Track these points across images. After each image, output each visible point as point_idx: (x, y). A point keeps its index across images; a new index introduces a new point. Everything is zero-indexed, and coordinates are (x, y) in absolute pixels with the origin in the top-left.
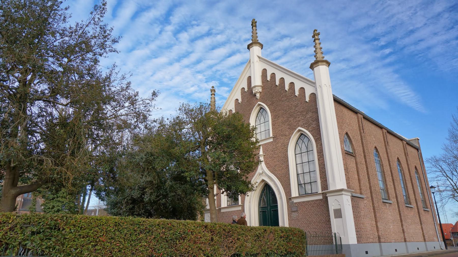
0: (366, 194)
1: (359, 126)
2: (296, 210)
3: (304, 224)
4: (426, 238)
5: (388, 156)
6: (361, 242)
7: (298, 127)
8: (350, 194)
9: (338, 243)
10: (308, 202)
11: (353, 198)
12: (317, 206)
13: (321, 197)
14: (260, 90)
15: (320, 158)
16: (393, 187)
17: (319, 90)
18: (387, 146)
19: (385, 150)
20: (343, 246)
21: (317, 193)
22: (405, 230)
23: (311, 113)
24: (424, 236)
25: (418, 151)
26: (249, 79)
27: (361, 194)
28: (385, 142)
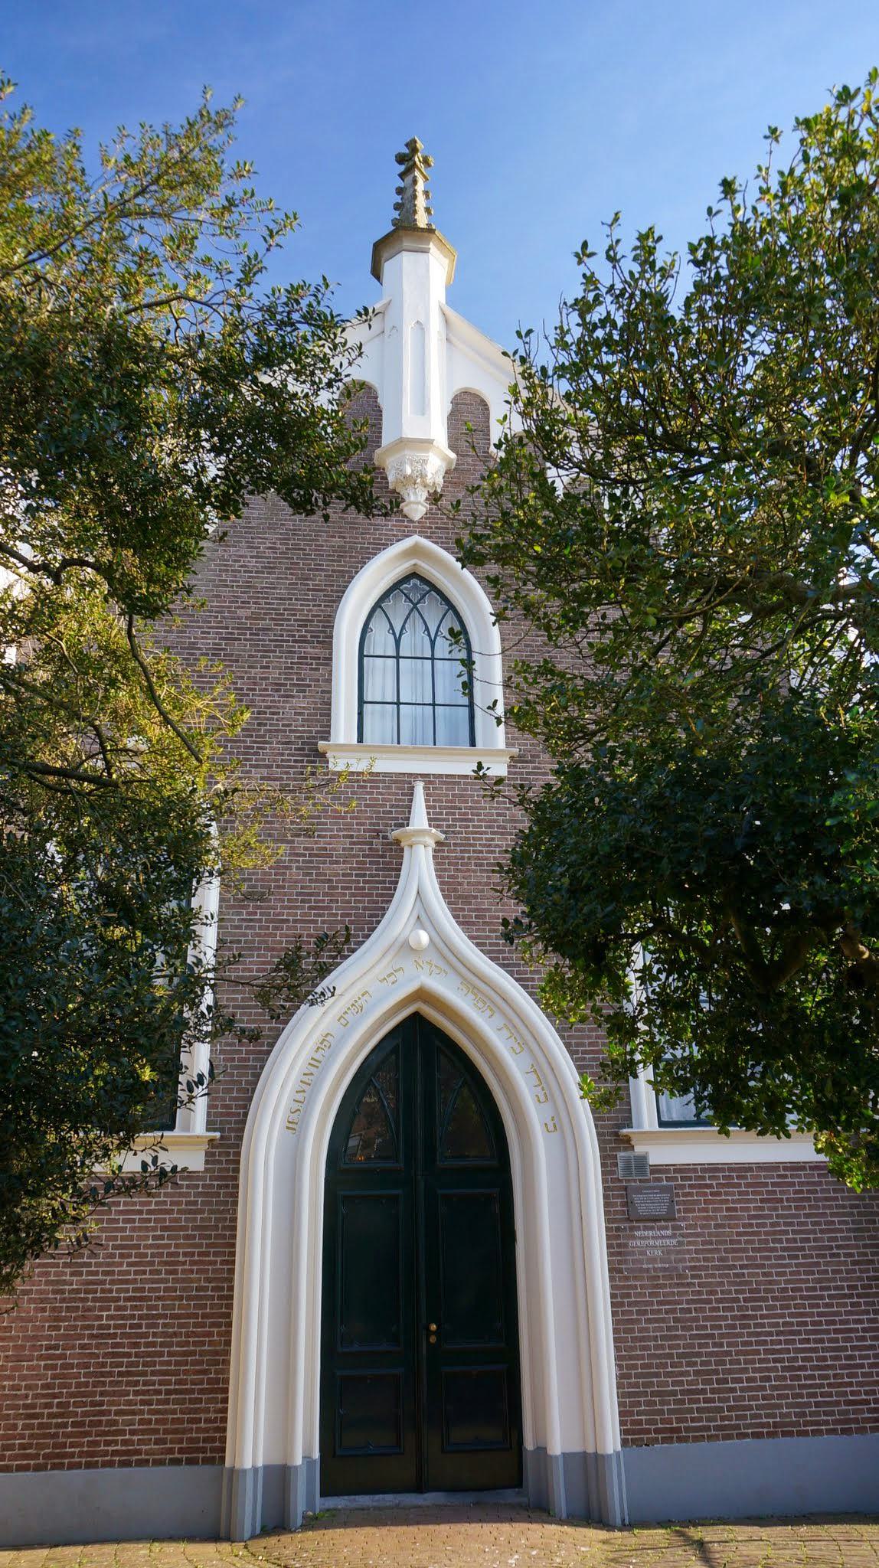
2: (663, 1210)
3: (719, 1301)
10: (742, 1169)
12: (795, 1200)
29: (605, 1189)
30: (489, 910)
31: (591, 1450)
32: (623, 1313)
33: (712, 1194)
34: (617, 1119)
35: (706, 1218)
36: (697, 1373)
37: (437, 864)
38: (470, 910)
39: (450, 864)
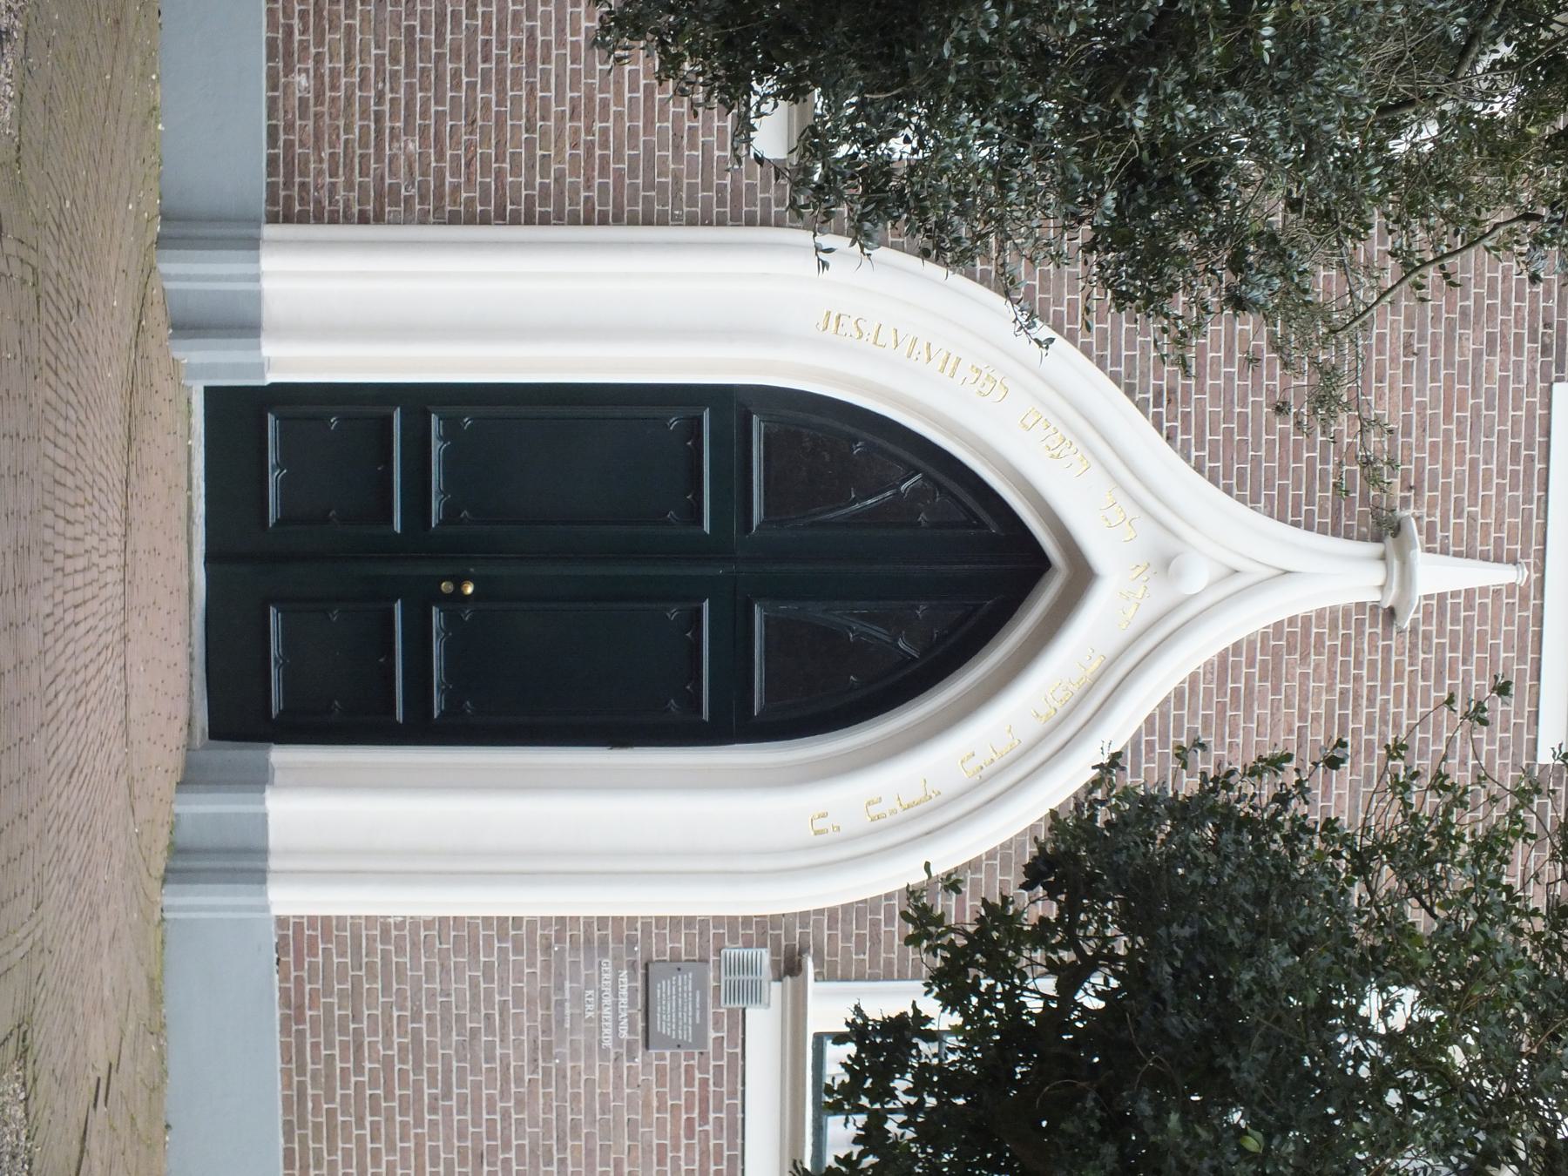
2: (663, 1024)
3: (506, 1114)
29: (704, 922)
30: (1248, 719)
31: (273, 863)
32: (488, 939)
33: (690, 1121)
34: (833, 953)
35: (647, 1105)
36: (388, 1062)
37: (1347, 611)
38: (1249, 677)
39: (1346, 637)
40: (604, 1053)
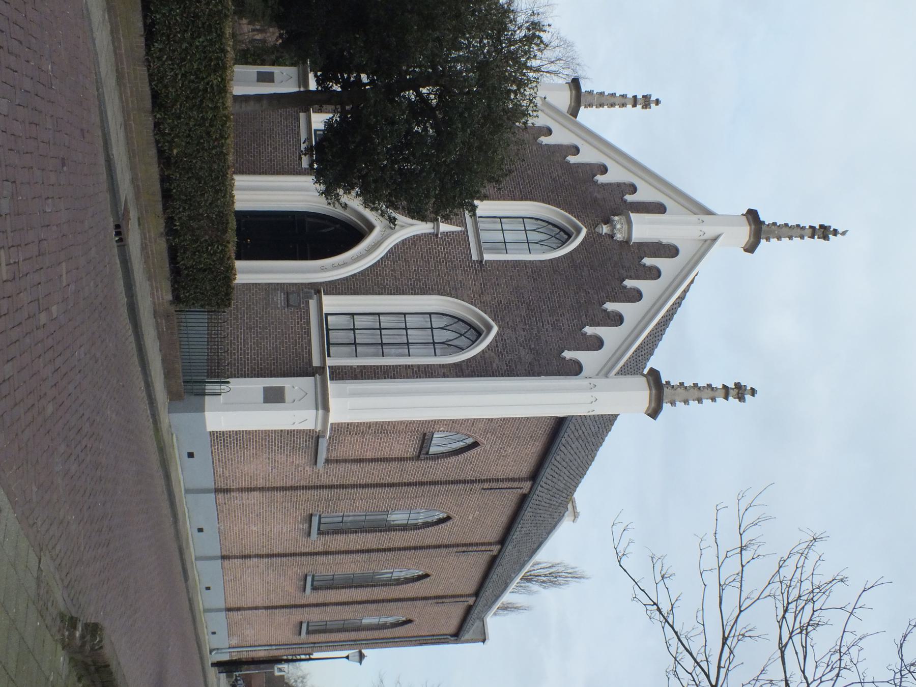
0: (323, 473)
1: (497, 480)
2: (291, 302)
4: (235, 613)
5: (429, 547)
6: (214, 443)
7: (499, 327)
8: (319, 428)
9: (209, 388)
10: (308, 333)
11: (315, 438)
12: (296, 351)
13: (316, 362)
14: (619, 237)
15: (413, 369)
16: (351, 548)
17: (586, 382)
18: (455, 549)
19: (445, 542)
20: (202, 397)
21: (329, 356)
22: (249, 562)
23: (530, 360)
24: (239, 609)
25: (452, 636)
26: (659, 208)
27: (327, 461)
28: (466, 545)
40: (279, 308)
